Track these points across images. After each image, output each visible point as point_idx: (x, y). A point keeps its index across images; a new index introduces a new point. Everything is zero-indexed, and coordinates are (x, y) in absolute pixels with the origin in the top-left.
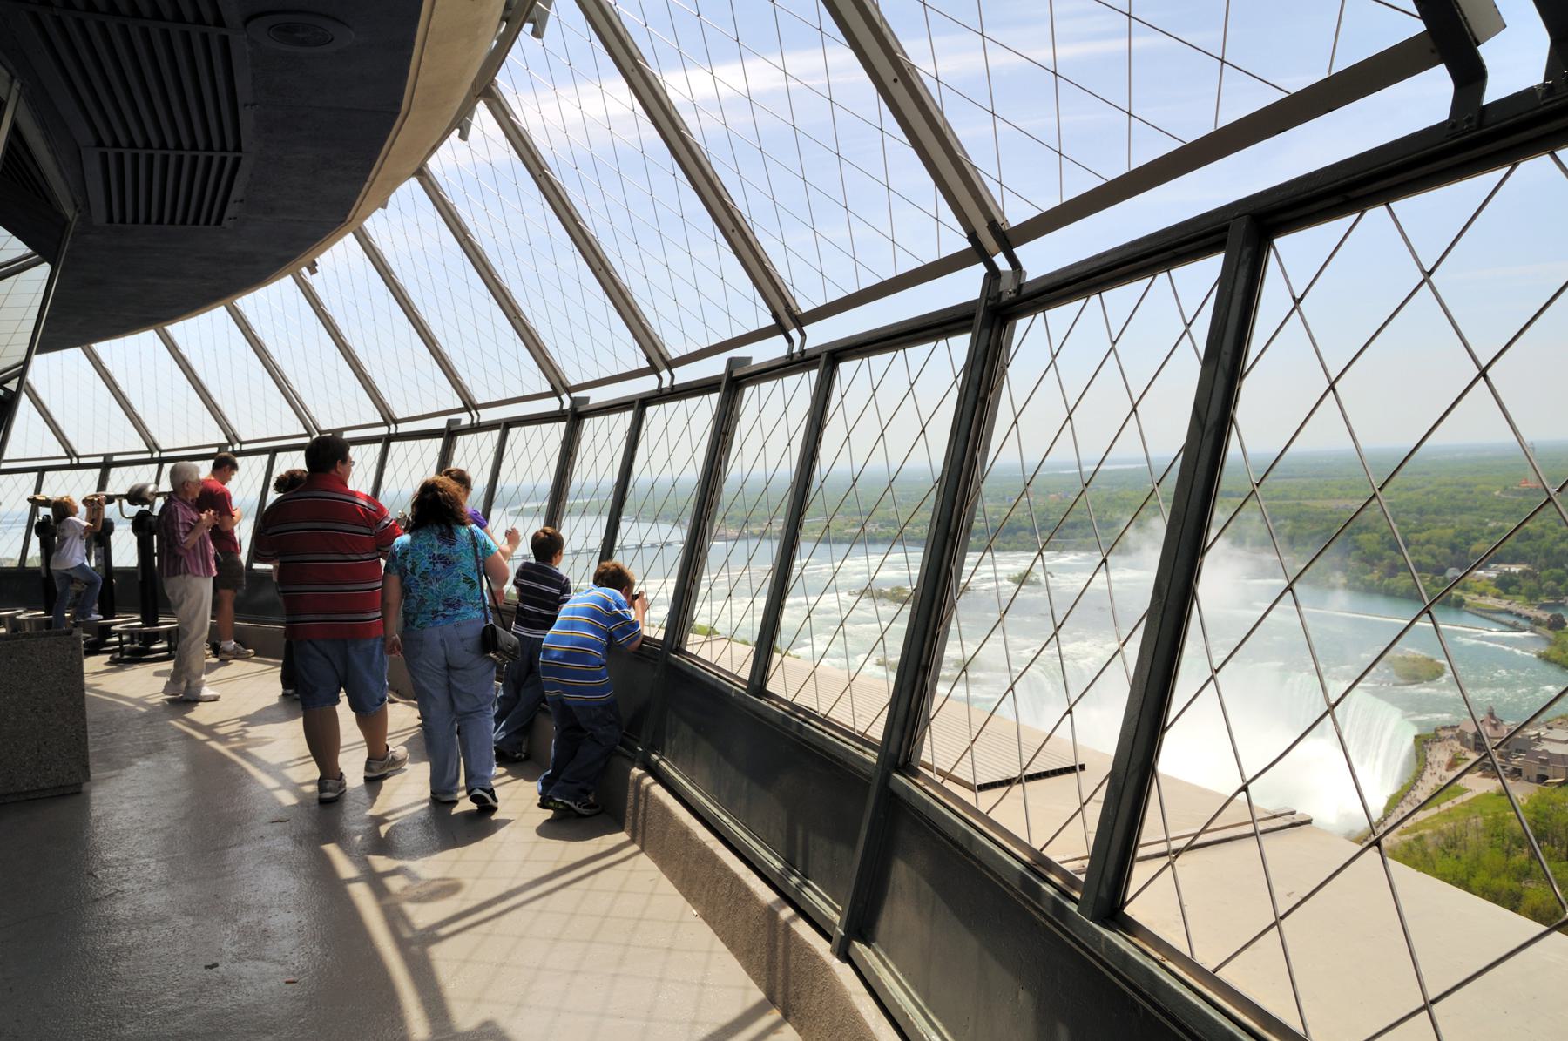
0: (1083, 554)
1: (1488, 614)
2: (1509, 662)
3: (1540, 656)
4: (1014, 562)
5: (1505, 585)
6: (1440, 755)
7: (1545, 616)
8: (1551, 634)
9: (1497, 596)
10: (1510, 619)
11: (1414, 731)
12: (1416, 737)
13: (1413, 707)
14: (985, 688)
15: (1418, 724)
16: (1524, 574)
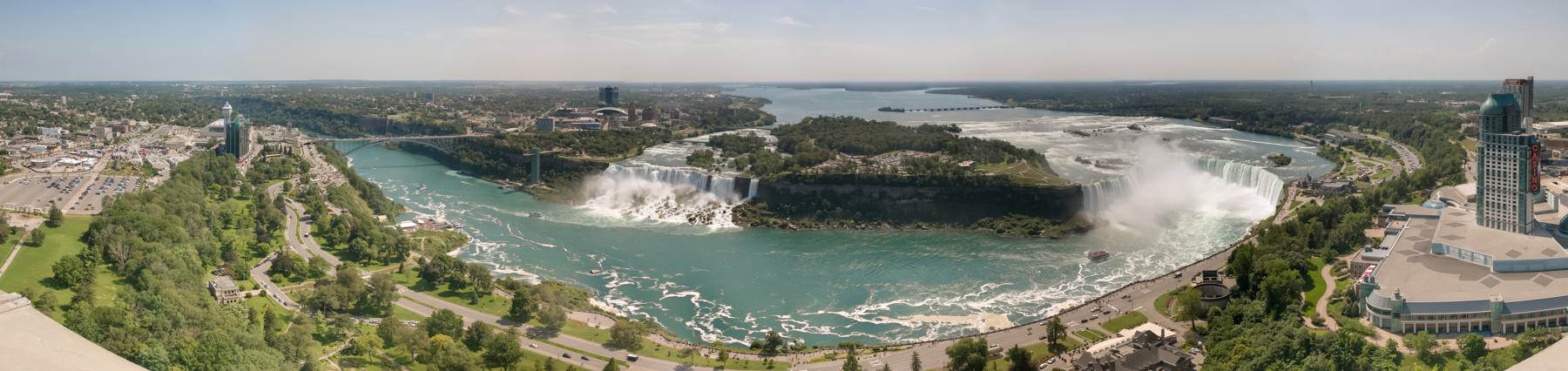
0: (1156, 118)
1: (1303, 141)
2: (1310, 157)
3: (1318, 154)
4: (1130, 120)
5: (1306, 131)
6: (1293, 189)
7: (1319, 140)
8: (1322, 147)
9: (1305, 134)
10: (1309, 143)
11: (1283, 183)
12: (1284, 187)
13: (1280, 175)
14: (1121, 171)
15: (1284, 180)
16: (1312, 127)
